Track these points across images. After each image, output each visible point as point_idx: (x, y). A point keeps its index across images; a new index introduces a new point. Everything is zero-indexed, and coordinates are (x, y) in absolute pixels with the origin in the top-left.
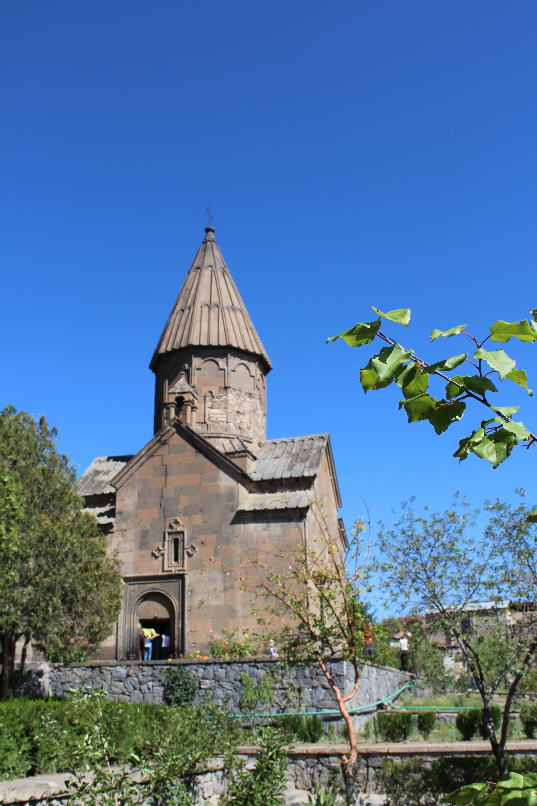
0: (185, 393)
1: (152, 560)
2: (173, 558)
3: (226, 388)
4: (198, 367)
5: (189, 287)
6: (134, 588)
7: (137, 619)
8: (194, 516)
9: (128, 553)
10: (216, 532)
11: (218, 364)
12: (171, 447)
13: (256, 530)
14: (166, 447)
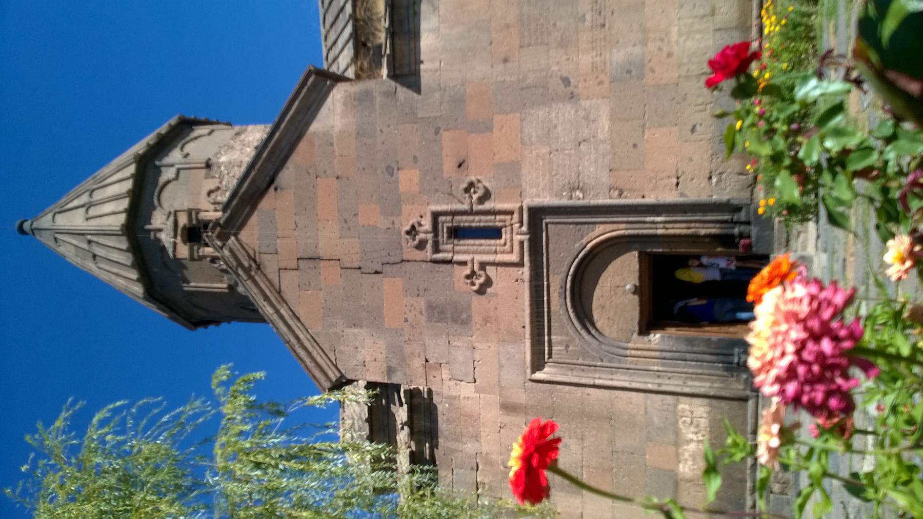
0: (176, 223)
1: (495, 295)
2: (493, 242)
3: (208, 165)
4: (165, 217)
5: (72, 248)
6: (560, 343)
7: (637, 341)
8: (401, 189)
9: (477, 356)
10: (437, 132)
11: (168, 182)
12: (264, 249)
13: (436, 30)
14: (265, 259)
